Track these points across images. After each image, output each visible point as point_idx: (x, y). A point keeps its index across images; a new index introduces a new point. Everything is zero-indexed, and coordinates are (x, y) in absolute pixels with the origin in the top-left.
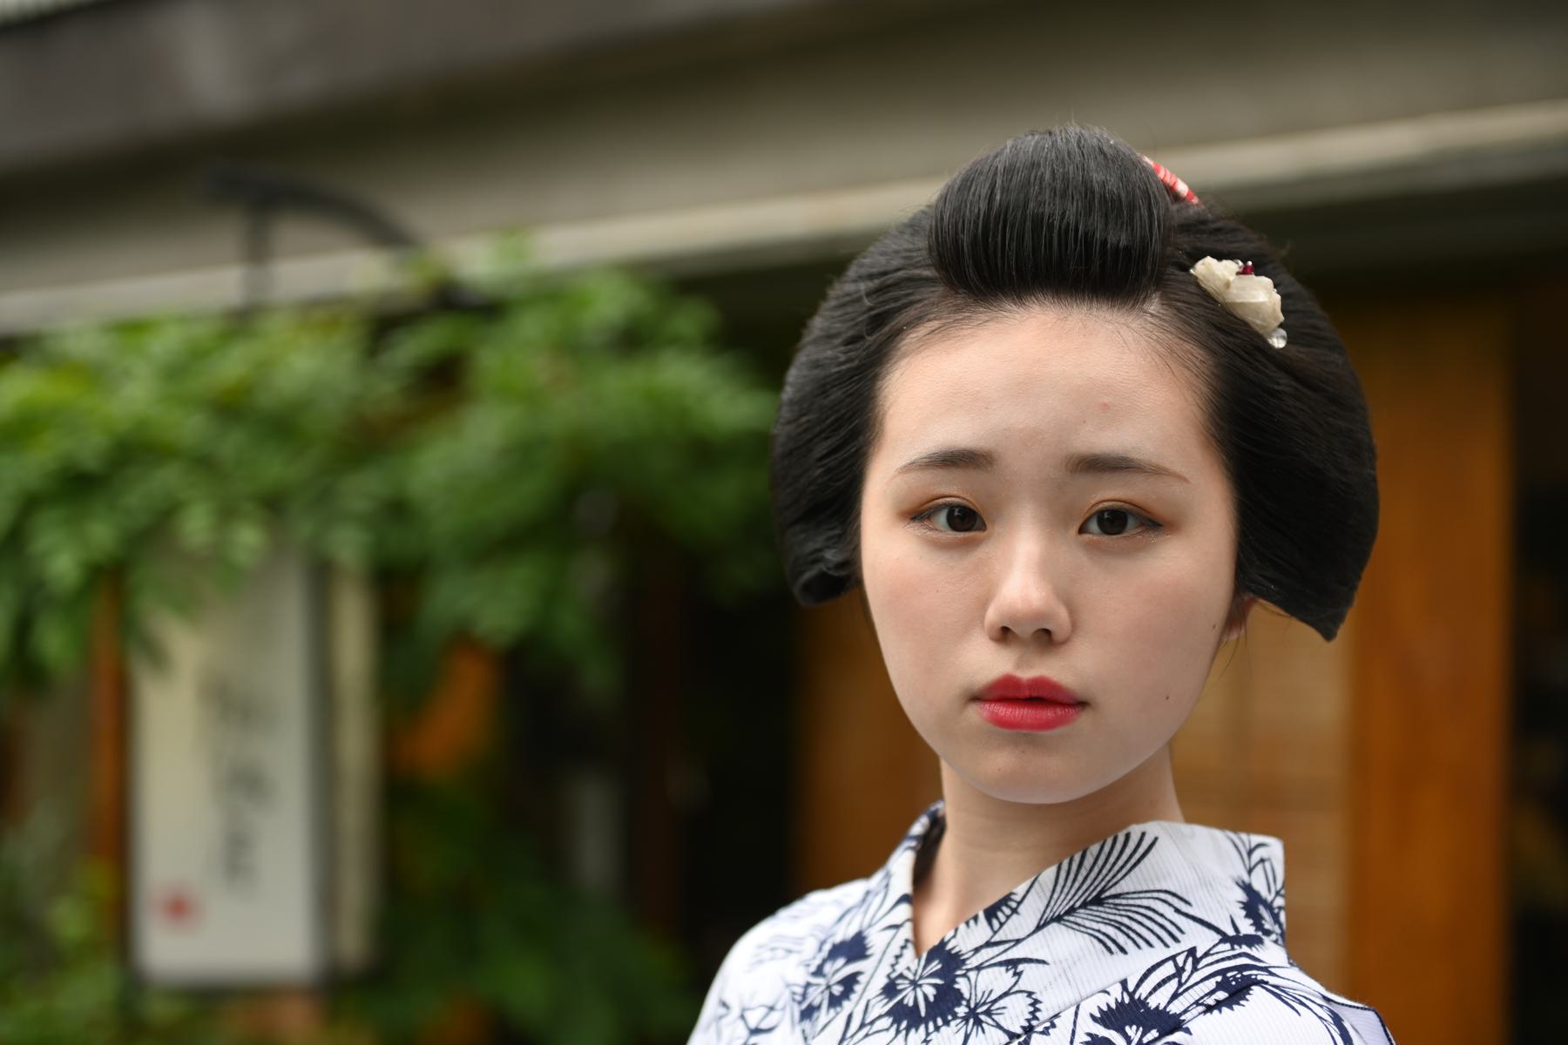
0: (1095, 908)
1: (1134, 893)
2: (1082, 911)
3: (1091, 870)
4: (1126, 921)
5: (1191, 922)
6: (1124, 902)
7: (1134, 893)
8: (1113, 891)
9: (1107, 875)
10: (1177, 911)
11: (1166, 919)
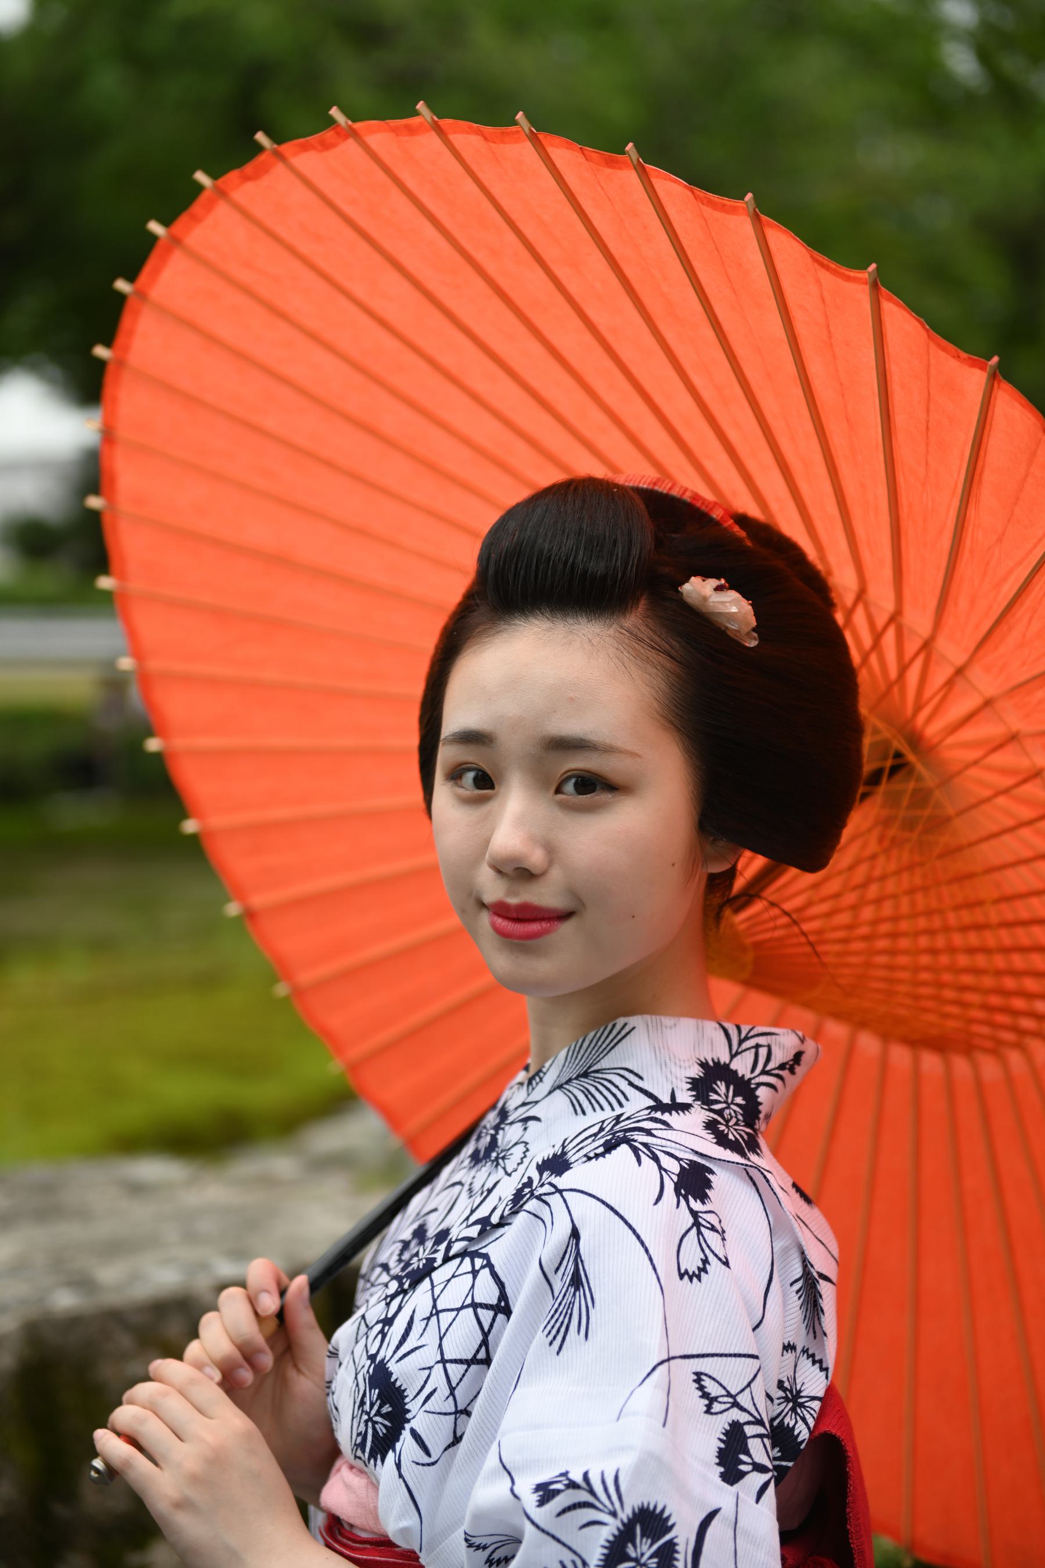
0: (582, 1079)
1: (608, 1069)
2: (575, 1081)
3: (586, 1050)
4: (593, 1090)
5: (637, 1093)
6: (600, 1076)
7: (608, 1069)
8: (595, 1068)
9: (594, 1054)
10: (631, 1084)
11: (619, 1090)
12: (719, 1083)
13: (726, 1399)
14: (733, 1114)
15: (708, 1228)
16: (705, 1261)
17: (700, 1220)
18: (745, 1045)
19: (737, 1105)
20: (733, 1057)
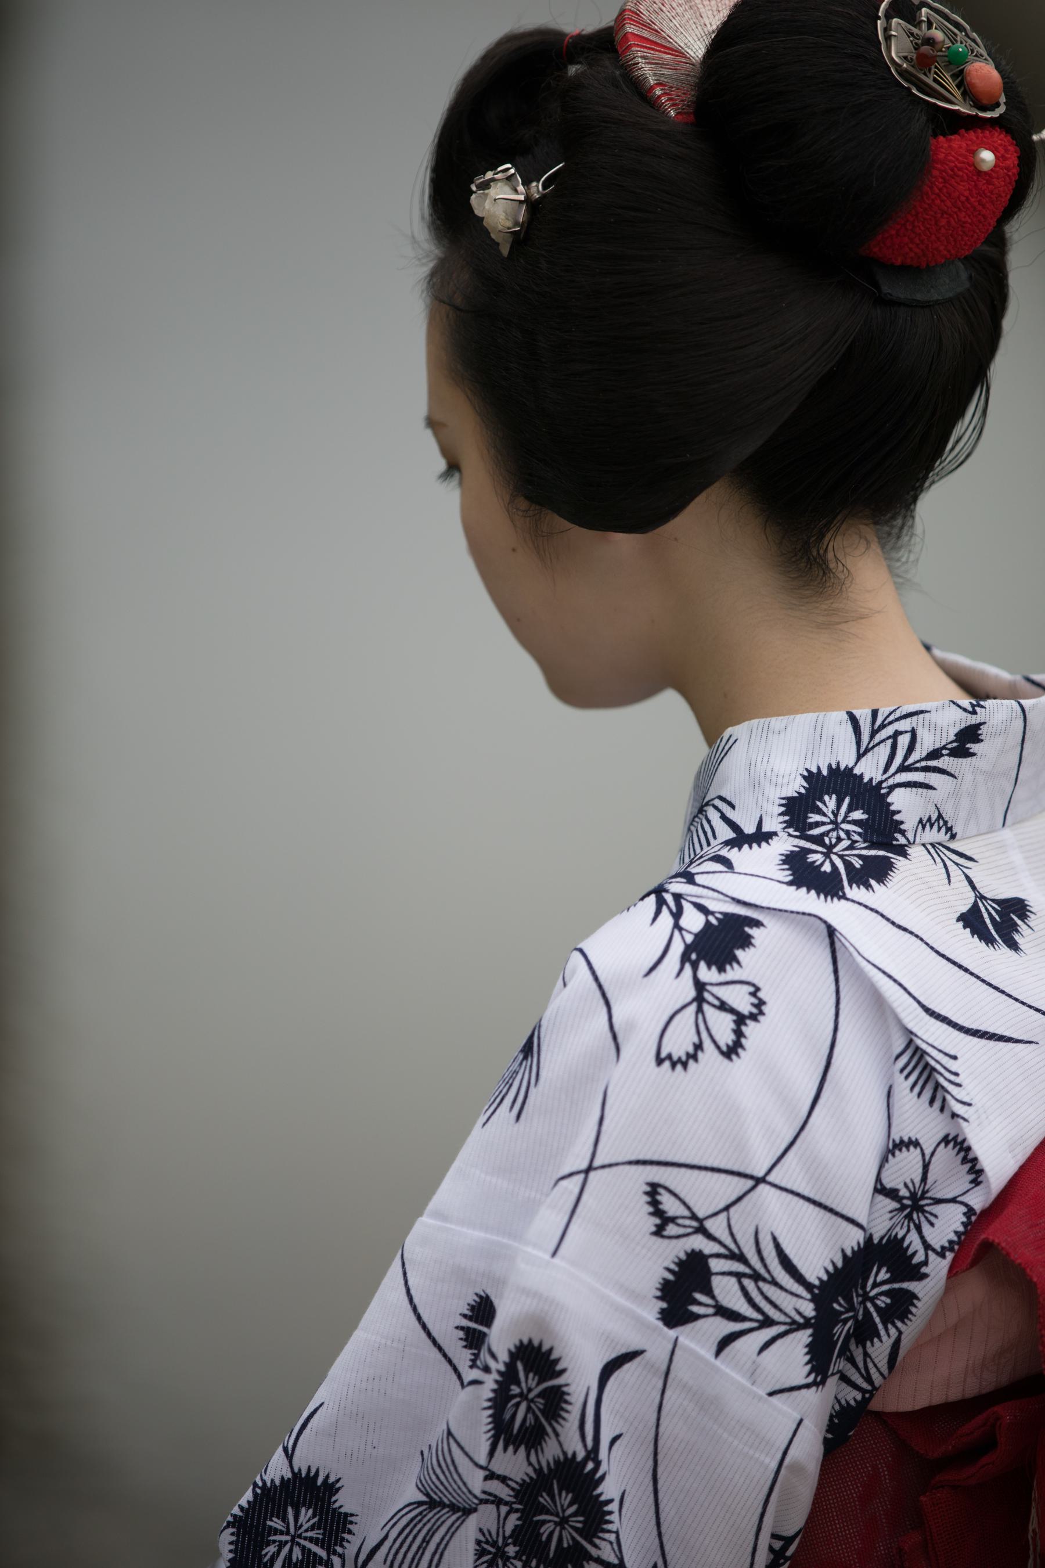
12: (826, 798)
13: (687, 1222)
14: (843, 835)
15: (714, 1006)
16: (699, 1047)
17: (706, 995)
18: (878, 738)
19: (855, 822)
20: (860, 756)
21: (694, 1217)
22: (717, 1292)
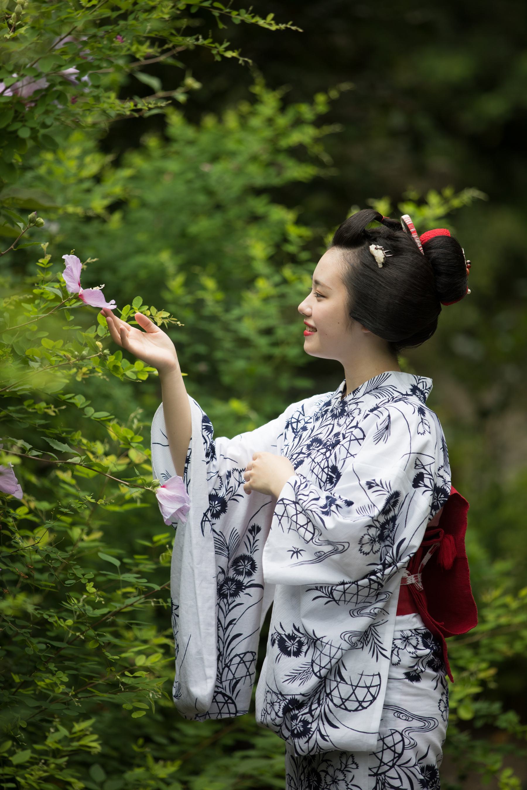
10: (393, 390)
21: (422, 465)
22: (425, 481)
